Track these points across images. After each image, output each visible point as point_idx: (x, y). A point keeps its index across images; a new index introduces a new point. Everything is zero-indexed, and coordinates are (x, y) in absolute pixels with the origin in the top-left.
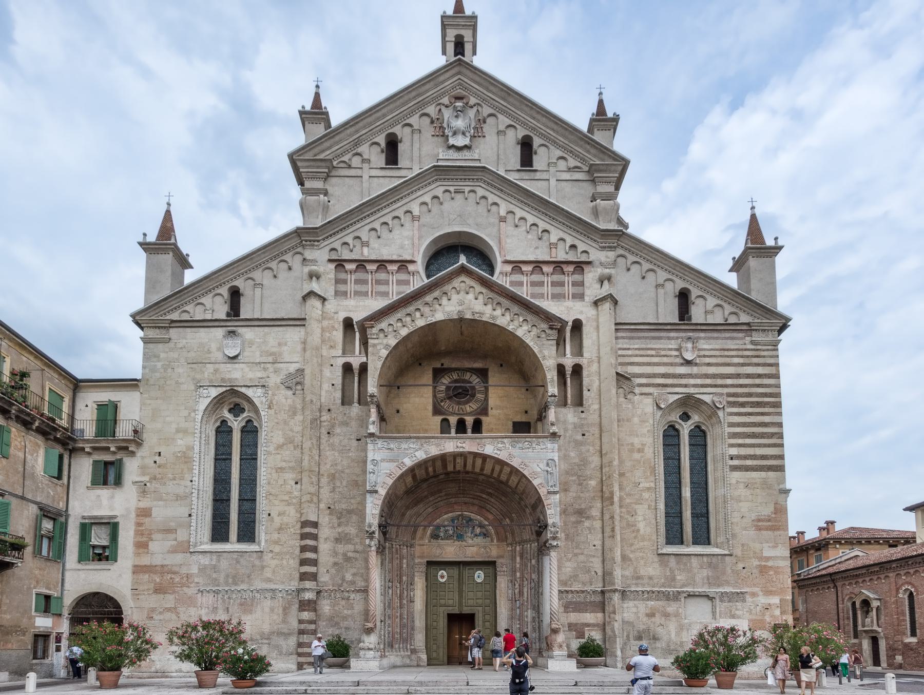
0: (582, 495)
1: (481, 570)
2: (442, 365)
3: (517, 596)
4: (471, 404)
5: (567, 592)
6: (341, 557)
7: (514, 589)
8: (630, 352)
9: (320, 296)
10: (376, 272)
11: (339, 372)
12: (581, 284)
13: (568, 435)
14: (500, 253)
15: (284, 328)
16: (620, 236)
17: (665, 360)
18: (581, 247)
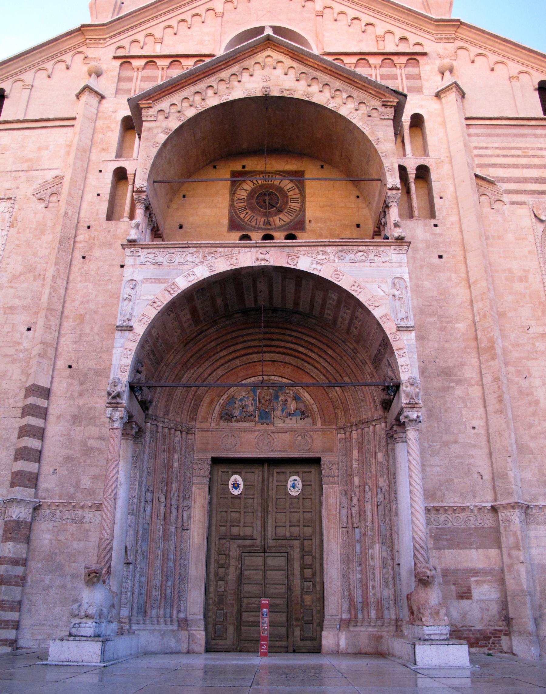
0: (446, 345)
1: (297, 473)
2: (244, 167)
3: (356, 520)
4: (281, 216)
5: (437, 510)
6: (77, 448)
7: (350, 507)
8: (489, 152)
9: (96, 93)
10: (168, 68)
11: (108, 178)
12: (418, 77)
13: (418, 257)
14: (317, 47)
15: (48, 130)
16: (459, 27)
17: (536, 161)
18: (413, 39)
